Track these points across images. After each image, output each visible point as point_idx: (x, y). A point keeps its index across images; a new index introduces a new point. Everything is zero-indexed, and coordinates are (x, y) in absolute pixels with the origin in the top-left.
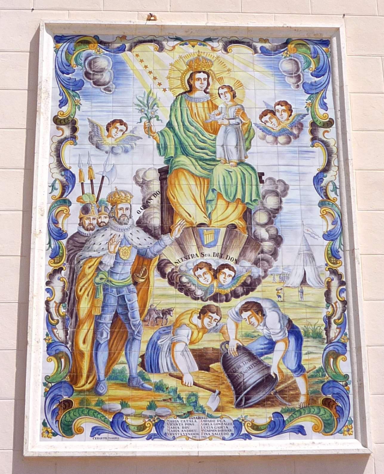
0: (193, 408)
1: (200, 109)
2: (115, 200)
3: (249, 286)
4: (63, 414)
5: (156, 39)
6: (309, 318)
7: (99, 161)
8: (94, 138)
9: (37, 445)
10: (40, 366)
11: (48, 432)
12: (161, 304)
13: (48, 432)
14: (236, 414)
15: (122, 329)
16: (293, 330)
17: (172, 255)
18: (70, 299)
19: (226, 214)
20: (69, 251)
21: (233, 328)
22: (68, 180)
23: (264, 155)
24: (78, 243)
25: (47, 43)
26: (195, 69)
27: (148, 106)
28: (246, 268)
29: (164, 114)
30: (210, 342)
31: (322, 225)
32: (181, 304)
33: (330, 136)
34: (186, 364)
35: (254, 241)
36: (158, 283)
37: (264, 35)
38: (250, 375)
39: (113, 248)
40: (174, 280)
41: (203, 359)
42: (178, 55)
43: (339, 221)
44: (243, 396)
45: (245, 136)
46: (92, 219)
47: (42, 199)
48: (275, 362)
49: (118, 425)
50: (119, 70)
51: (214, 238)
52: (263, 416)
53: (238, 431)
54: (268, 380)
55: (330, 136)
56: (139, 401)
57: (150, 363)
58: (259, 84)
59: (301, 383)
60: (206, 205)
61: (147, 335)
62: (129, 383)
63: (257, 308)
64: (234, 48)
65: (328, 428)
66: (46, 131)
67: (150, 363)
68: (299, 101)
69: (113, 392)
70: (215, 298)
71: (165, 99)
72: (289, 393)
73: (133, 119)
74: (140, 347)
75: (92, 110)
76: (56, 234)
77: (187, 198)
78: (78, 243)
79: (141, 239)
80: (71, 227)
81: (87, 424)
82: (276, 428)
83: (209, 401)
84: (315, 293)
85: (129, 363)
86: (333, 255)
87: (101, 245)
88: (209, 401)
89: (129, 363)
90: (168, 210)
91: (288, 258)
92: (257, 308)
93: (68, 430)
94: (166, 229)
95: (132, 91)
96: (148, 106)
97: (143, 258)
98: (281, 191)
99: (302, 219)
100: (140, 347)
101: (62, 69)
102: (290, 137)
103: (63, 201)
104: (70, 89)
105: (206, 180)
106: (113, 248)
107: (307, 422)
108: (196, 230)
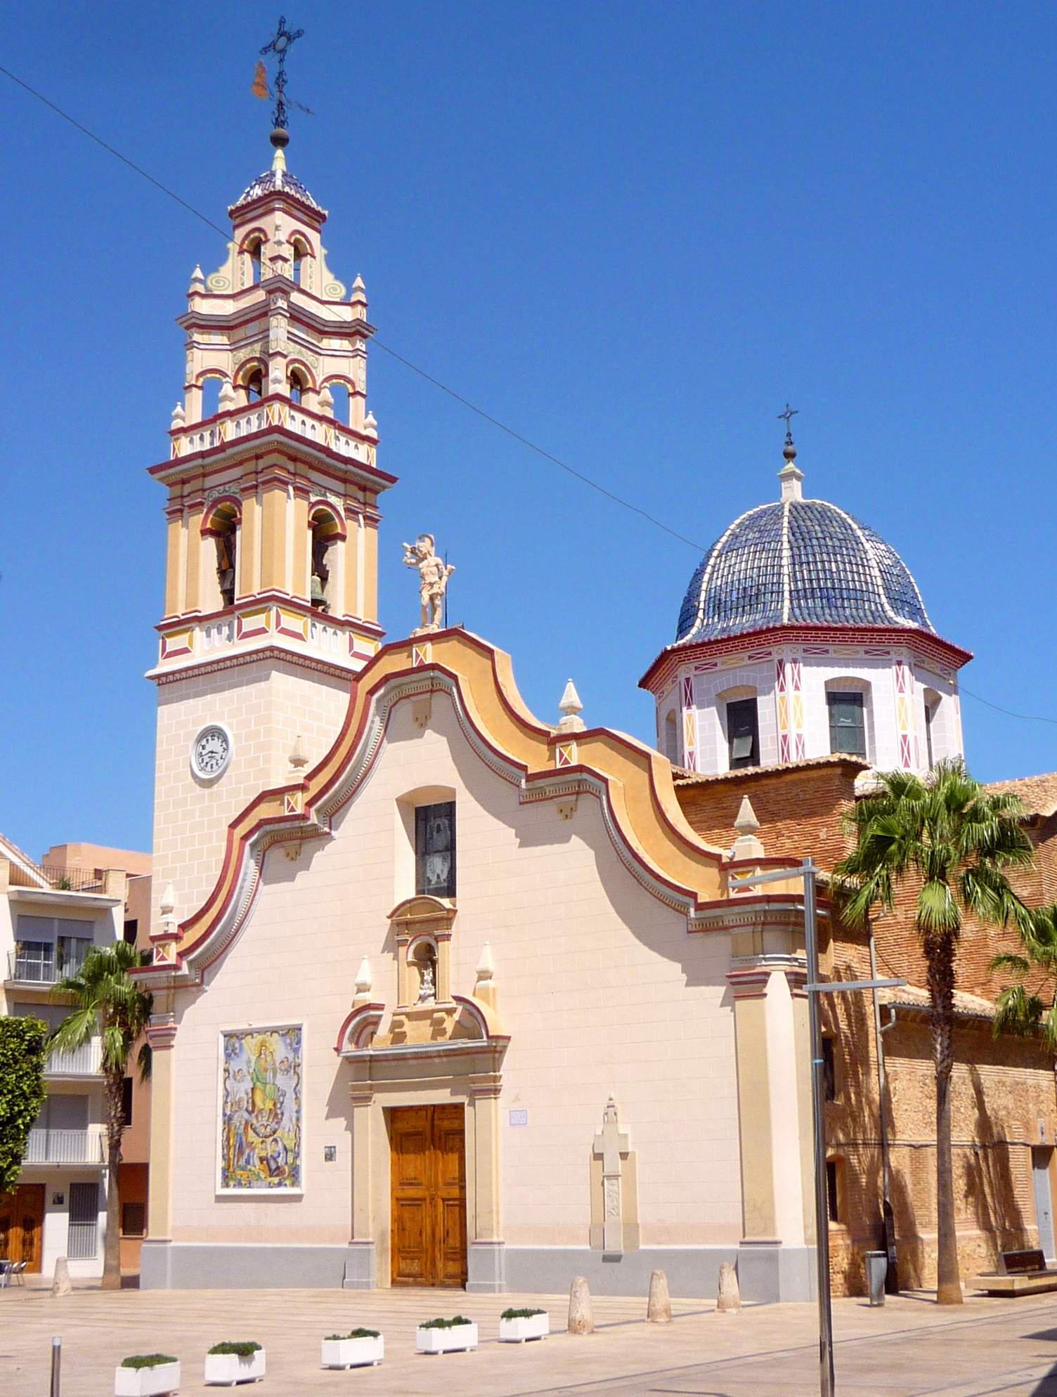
0: (259, 1178)
1: (263, 1062)
2: (240, 1100)
3: (274, 1132)
5: (250, 1033)
6: (290, 1145)
7: (236, 1084)
10: (220, 1164)
12: (250, 1140)
14: (270, 1179)
15: (241, 1151)
16: (285, 1148)
18: (228, 1139)
19: (269, 1105)
20: (228, 1120)
21: (270, 1149)
25: (221, 1037)
26: (263, 1044)
28: (274, 1125)
29: (253, 1064)
30: (263, 1154)
31: (295, 1108)
33: (298, 1070)
34: (257, 1162)
35: (276, 1115)
36: (251, 1132)
37: (282, 1028)
38: (273, 1166)
39: (240, 1118)
41: (262, 1159)
42: (259, 1038)
43: (299, 1106)
44: (272, 1173)
46: (235, 1108)
48: (280, 1160)
49: (240, 1185)
51: (266, 1114)
52: (276, 1180)
53: (270, 1186)
54: (278, 1168)
55: (298, 1070)
57: (248, 1162)
58: (279, 1048)
59: (287, 1169)
60: (264, 1102)
61: (247, 1151)
62: (243, 1169)
63: (275, 1140)
64: (275, 1035)
65: (293, 1184)
67: (248, 1162)
69: (239, 1172)
70: (266, 1137)
71: (253, 1058)
72: (283, 1172)
74: (245, 1156)
75: (234, 1066)
76: (225, 1115)
78: (230, 1118)
79: (246, 1115)
80: (228, 1113)
82: (279, 1184)
83: (262, 1175)
84: (292, 1135)
85: (242, 1162)
87: (235, 1120)
88: (262, 1175)
89: (242, 1162)
92: (275, 1140)
93: (227, 1186)
94: (253, 1111)
95: (244, 1057)
96: (249, 1062)
100: (245, 1156)
101: (226, 1049)
103: (226, 1102)
104: (228, 1056)
105: (264, 1091)
106: (240, 1118)
107: (288, 1182)
108: (261, 1111)
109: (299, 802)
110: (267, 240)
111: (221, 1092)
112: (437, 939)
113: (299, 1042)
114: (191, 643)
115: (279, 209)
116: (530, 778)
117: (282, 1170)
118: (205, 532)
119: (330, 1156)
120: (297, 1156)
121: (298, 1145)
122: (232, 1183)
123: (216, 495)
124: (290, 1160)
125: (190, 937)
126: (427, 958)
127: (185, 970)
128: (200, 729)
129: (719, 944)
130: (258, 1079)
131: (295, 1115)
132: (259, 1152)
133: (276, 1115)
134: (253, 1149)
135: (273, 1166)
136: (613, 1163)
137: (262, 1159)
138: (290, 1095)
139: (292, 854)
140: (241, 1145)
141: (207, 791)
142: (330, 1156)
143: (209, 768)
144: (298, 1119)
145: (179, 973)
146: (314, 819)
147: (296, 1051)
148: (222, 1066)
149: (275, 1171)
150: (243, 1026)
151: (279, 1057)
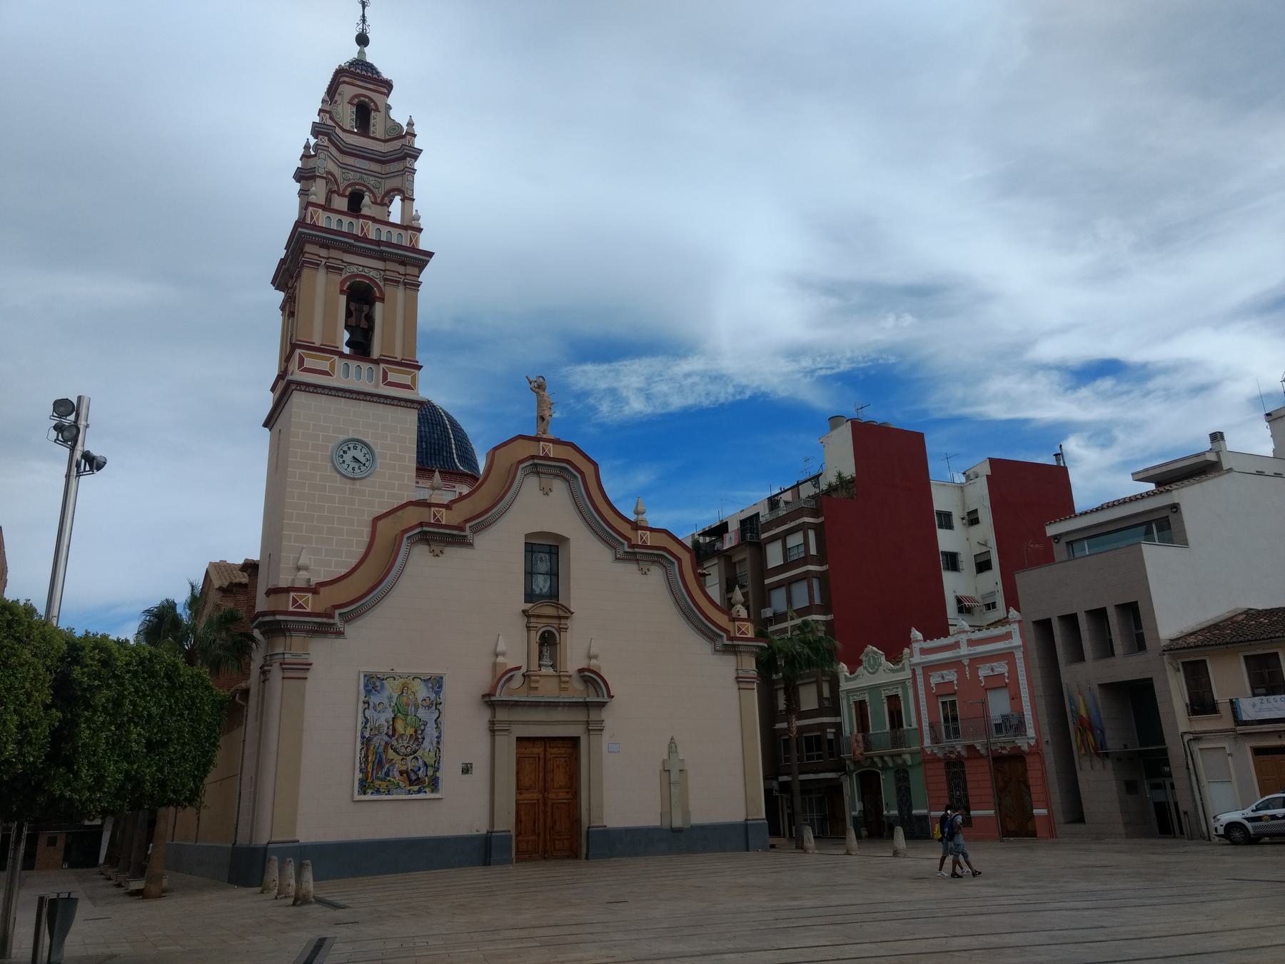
4: (363, 790)
6: (430, 761)
8: (374, 708)
9: (358, 797)
10: (358, 775)
11: (359, 793)
13: (359, 793)
15: (380, 764)
16: (425, 764)
17: (395, 743)
18: (366, 756)
19: (410, 731)
20: (366, 742)
21: (410, 764)
22: (367, 721)
23: (422, 713)
24: (369, 740)
27: (390, 698)
29: (394, 700)
30: (404, 768)
32: (397, 758)
33: (440, 707)
34: (396, 774)
35: (417, 739)
36: (390, 751)
38: (414, 777)
40: (395, 750)
41: (401, 773)
44: (411, 783)
45: (417, 708)
47: (360, 727)
49: (378, 792)
50: (382, 685)
52: (416, 788)
53: (409, 792)
54: (418, 779)
55: (440, 707)
56: (384, 784)
57: (387, 774)
58: (422, 692)
66: (361, 706)
67: (387, 774)
68: (433, 696)
71: (395, 696)
73: (386, 701)
75: (374, 699)
76: (363, 737)
77: (400, 726)
78: (369, 740)
79: (386, 738)
81: (370, 791)
82: (419, 791)
84: (432, 754)
86: (438, 743)
90: (394, 730)
91: (426, 743)
93: (365, 793)
95: (386, 694)
96: (390, 698)
97: (387, 743)
98: (425, 724)
99: (431, 731)
101: (366, 686)
102: (429, 707)
104: (368, 692)
109: (445, 517)
110: (377, 110)
111: (361, 719)
112: (559, 630)
113: (440, 687)
114: (332, 365)
115: (344, 82)
116: (632, 546)
117: (423, 780)
118: (342, 292)
119: (466, 770)
120: (437, 770)
121: (438, 761)
122: (370, 791)
123: (354, 269)
124: (430, 772)
125: (328, 598)
126: (548, 641)
127: (337, 620)
128: (343, 437)
129: (731, 659)
130: (400, 711)
131: (435, 740)
132: (399, 766)
133: (418, 738)
134: (393, 765)
135: (414, 777)
136: (675, 776)
137: (401, 773)
138: (431, 724)
139: (437, 551)
140: (380, 762)
141: (348, 485)
142: (466, 770)
143: (350, 469)
144: (438, 743)
145: (331, 621)
146: (467, 532)
147: (437, 693)
148: (362, 698)
149: (418, 781)
150: (385, 669)
151: (420, 698)
